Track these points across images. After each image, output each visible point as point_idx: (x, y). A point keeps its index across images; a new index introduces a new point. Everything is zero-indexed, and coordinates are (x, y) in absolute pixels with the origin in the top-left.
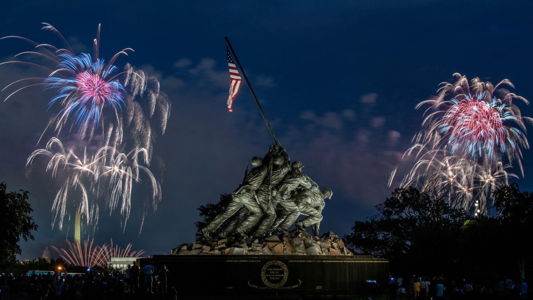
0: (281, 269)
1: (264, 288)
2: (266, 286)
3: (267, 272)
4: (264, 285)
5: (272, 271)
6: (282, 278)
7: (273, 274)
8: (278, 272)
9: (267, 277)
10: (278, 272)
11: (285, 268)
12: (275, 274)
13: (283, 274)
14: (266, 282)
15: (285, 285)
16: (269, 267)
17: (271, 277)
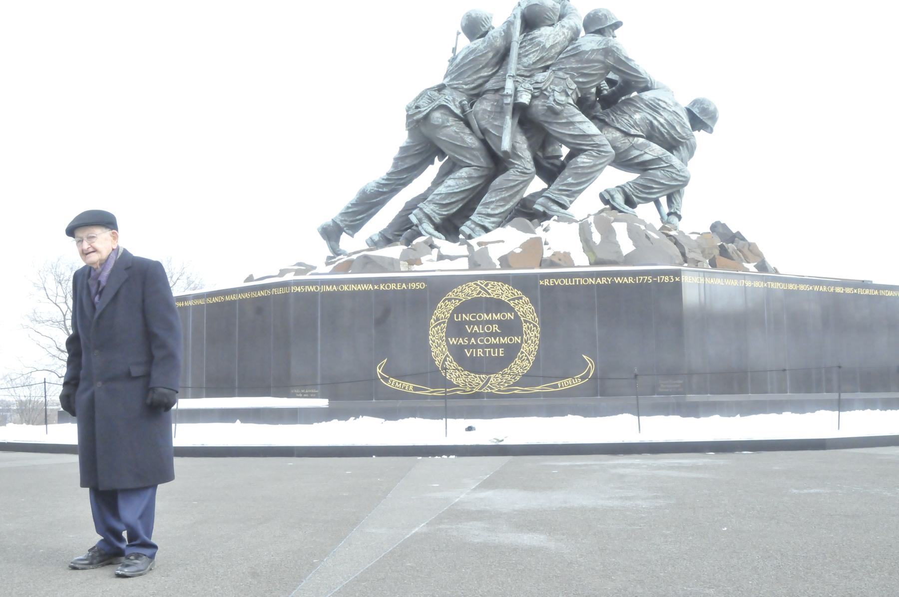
0: (509, 316)
2: (448, 384)
3: (456, 328)
5: (477, 323)
6: (512, 351)
7: (476, 335)
8: (495, 328)
9: (451, 348)
10: (495, 328)
11: (525, 308)
13: (520, 333)
15: (529, 379)
16: (458, 310)
17: (469, 347)
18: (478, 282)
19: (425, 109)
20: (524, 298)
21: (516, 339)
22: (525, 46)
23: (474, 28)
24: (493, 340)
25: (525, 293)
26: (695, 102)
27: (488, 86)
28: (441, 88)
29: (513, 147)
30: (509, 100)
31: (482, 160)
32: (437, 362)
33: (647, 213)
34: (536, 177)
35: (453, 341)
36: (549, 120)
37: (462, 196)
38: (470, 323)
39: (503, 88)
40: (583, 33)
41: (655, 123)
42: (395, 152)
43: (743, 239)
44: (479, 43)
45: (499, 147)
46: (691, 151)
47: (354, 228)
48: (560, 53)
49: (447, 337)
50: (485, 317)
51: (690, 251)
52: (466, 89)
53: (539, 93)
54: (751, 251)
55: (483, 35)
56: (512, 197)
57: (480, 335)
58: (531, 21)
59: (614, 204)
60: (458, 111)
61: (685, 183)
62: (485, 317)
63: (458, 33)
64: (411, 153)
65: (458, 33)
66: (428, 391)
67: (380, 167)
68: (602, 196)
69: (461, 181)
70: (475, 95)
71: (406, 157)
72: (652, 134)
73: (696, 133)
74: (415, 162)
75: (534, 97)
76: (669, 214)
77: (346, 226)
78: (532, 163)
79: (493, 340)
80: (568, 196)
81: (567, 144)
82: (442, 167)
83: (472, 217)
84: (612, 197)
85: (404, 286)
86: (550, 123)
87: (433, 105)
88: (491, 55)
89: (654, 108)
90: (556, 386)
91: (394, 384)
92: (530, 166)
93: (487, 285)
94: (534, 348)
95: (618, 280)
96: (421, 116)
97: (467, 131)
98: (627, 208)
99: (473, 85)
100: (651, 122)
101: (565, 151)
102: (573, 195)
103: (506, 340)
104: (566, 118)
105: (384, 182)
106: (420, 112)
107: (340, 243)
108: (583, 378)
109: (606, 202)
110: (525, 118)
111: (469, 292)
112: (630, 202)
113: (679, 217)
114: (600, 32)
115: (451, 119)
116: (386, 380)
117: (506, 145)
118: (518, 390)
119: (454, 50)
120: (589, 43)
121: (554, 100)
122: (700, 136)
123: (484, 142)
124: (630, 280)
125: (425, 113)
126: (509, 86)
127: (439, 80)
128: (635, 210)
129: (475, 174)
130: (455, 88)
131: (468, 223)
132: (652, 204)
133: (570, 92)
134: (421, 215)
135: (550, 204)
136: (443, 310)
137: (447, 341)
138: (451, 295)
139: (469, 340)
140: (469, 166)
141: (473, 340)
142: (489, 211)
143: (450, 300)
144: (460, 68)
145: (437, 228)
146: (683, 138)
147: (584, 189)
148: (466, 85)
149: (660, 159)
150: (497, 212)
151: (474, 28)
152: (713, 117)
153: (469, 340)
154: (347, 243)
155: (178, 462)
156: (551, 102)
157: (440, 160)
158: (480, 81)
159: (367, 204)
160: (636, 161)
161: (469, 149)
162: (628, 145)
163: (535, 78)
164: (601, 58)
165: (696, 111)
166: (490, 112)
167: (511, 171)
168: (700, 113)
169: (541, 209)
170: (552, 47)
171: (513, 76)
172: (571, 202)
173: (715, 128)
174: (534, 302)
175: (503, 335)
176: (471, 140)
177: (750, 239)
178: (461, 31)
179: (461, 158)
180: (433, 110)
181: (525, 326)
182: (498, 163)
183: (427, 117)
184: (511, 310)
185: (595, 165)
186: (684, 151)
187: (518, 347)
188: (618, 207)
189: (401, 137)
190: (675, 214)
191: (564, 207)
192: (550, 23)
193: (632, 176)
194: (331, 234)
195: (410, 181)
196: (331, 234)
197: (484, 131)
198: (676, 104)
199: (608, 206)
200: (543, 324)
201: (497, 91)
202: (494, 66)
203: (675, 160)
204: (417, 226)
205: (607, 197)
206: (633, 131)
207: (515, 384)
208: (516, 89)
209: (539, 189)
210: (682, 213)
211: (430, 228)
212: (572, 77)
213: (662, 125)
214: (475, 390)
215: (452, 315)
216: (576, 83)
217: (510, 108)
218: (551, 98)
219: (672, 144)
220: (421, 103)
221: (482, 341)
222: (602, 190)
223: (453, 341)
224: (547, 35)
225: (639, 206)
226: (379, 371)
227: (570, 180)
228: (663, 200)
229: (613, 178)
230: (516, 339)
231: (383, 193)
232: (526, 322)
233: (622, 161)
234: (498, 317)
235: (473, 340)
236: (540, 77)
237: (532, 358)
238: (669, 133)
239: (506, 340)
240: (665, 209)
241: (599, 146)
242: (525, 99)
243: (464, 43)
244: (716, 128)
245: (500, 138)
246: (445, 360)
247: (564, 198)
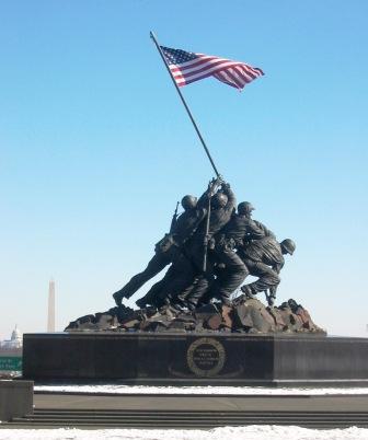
3: (196, 354)
6: (216, 362)
11: (220, 348)
25: (221, 342)
33: (261, 297)
67: (142, 267)
72: (265, 260)
89: (266, 248)
91: (177, 374)
112: (254, 293)
122: (286, 257)
136: (192, 348)
144: (178, 225)
152: (292, 249)
154: (126, 302)
155: (35, 396)
174: (224, 346)
196: (118, 296)
229: (251, 279)
233: (254, 271)
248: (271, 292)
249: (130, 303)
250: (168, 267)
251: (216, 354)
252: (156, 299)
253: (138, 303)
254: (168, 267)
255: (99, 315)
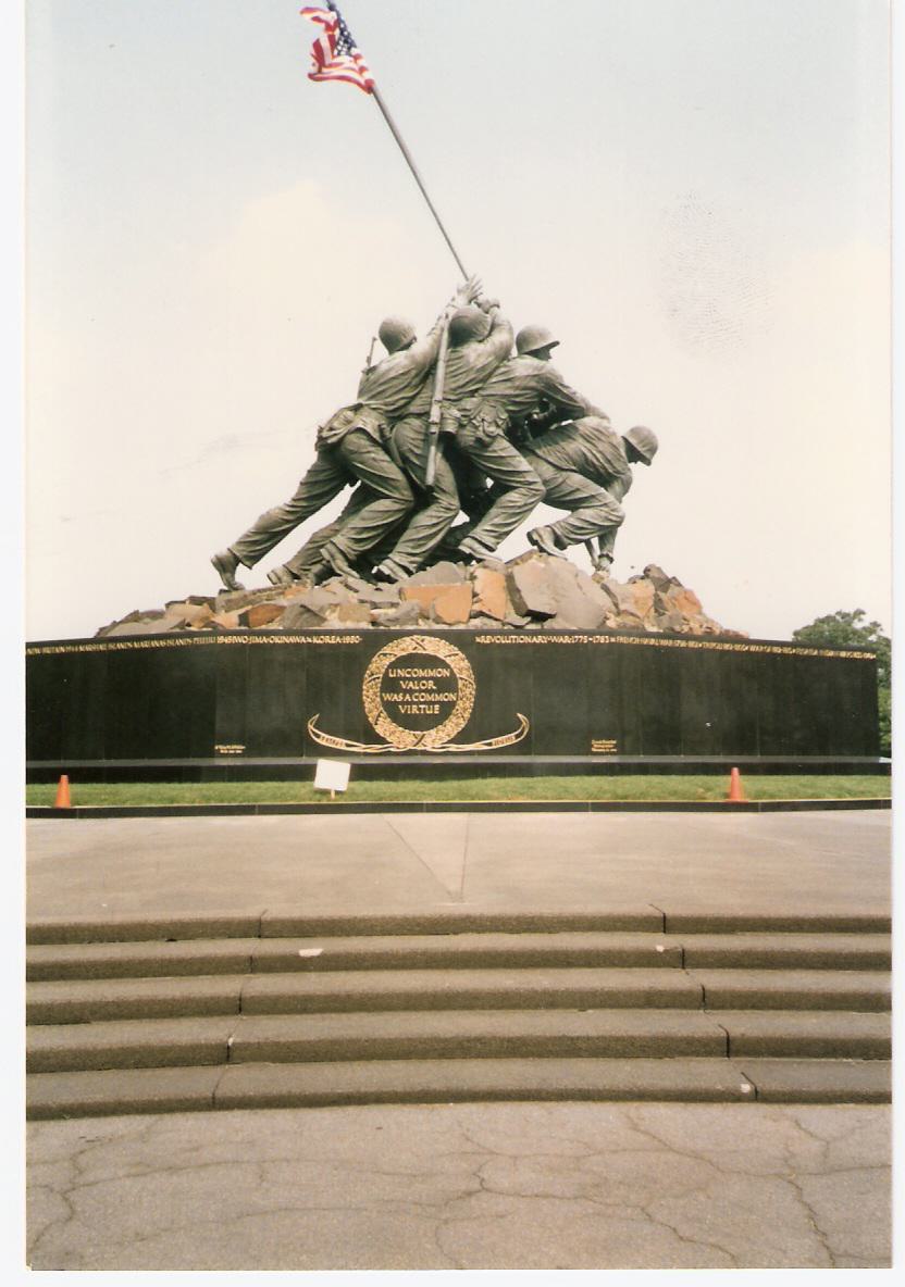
1: (375, 748)
2: (381, 740)
3: (390, 685)
4: (372, 737)
5: (412, 679)
6: (447, 709)
7: (411, 691)
11: (459, 664)
12: (420, 691)
13: (455, 690)
14: (384, 727)
15: (462, 737)
16: (393, 666)
17: (403, 703)
18: (415, 637)
19: (342, 431)
20: (461, 654)
21: (452, 697)
22: (452, 365)
23: (393, 339)
24: (429, 698)
26: (634, 431)
27: (413, 408)
28: (357, 408)
29: (437, 479)
30: (434, 429)
31: (407, 494)
32: (370, 719)
33: (577, 554)
34: (461, 512)
35: (387, 697)
36: (478, 452)
37: (380, 531)
38: (405, 679)
39: (427, 414)
40: (514, 352)
41: (589, 455)
42: (302, 474)
43: (679, 585)
44: (401, 358)
45: (423, 480)
46: (626, 486)
47: (253, 559)
48: (490, 375)
49: (381, 692)
50: (421, 673)
51: (623, 600)
52: (387, 412)
53: (465, 421)
54: (686, 598)
55: (407, 346)
56: (436, 534)
57: (416, 691)
58: (460, 333)
59: (543, 545)
60: (376, 436)
61: (619, 524)
62: (421, 673)
63: (375, 339)
64: (321, 477)
65: (375, 339)
66: (360, 748)
67: (283, 490)
68: (529, 535)
69: (379, 514)
70: (396, 416)
71: (311, 483)
73: (632, 465)
74: (326, 488)
75: (462, 426)
76: (600, 557)
77: (245, 556)
78: (457, 497)
79: (429, 698)
80: (496, 537)
81: (492, 478)
82: (354, 495)
83: (395, 556)
84: (540, 536)
85: (338, 639)
86: (476, 455)
87: (350, 427)
88: (413, 373)
90: (490, 744)
92: (456, 502)
93: (423, 641)
94: (469, 704)
95: (554, 639)
96: (334, 440)
97: (387, 458)
98: (556, 551)
99: (392, 408)
100: (584, 454)
101: (489, 483)
102: (501, 536)
103: (441, 697)
104: (495, 451)
105: (288, 509)
106: (335, 435)
107: (236, 576)
108: (517, 736)
109: (534, 543)
110: (448, 443)
111: (406, 646)
112: (560, 544)
113: (611, 560)
114: (535, 354)
115: (368, 443)
116: (318, 736)
117: (430, 480)
118: (453, 748)
119: (369, 360)
120: (524, 366)
121: (484, 431)
122: (637, 468)
123: (404, 471)
124: (566, 640)
125: (339, 436)
126: (435, 415)
127: (354, 400)
128: (564, 551)
129: (397, 507)
130: (374, 409)
131: (387, 561)
132: (583, 544)
133: (500, 423)
134: (334, 550)
135: (476, 546)
136: (379, 664)
137: (382, 698)
138: (386, 650)
139: (404, 696)
140: (388, 497)
141: (408, 697)
142: (410, 551)
143: (385, 655)
145: (352, 565)
146: (618, 472)
147: (512, 531)
148: (386, 405)
149: (593, 496)
150: (418, 551)
151: (393, 339)
152: (653, 450)
153: (404, 696)
154: (242, 574)
156: (480, 434)
157: (352, 486)
158: (403, 402)
159: (268, 535)
160: (568, 498)
161: (384, 480)
162: (560, 480)
163: (463, 403)
164: (533, 384)
165: (633, 441)
166: (413, 439)
167: (434, 507)
168: (639, 443)
169: (468, 551)
170: (483, 368)
171: (440, 402)
172: (498, 543)
173: (654, 460)
175: (439, 692)
176: (392, 471)
177: (687, 585)
178: (377, 337)
179: (380, 489)
180: (349, 433)
181: (460, 683)
182: (423, 497)
183: (341, 441)
184: (447, 666)
185: (526, 505)
186: (617, 487)
187: (452, 704)
188: (546, 548)
189: (311, 457)
190: (607, 556)
191: (491, 550)
192: (481, 338)
193: (563, 514)
194: (226, 566)
195: (319, 509)
197: (405, 460)
198: (614, 434)
199: (536, 547)
200: (478, 681)
201: (418, 415)
202: (416, 386)
203: (608, 496)
204: (328, 562)
205: (535, 537)
206: (564, 465)
207: (449, 742)
208: (442, 414)
209: (460, 523)
210: (614, 555)
211: (344, 566)
212: (504, 404)
213: (597, 459)
214: (409, 747)
215: (387, 670)
216: (508, 411)
217: (436, 436)
218: (481, 429)
219: (604, 478)
220: (336, 424)
221: (416, 697)
222: (530, 529)
223: (387, 697)
224: (476, 353)
225: (569, 547)
226: (310, 727)
227: (497, 521)
228: (595, 542)
229: (545, 516)
230: (452, 697)
231: (288, 521)
232: (461, 679)
233: (554, 499)
234: (432, 673)
235: (408, 697)
236: (469, 403)
237: (467, 715)
238: (605, 468)
239: (441, 697)
240: (597, 552)
241: (531, 483)
242: (451, 428)
243: (381, 351)
244: (654, 460)
245: (424, 470)
246: (379, 716)
247: (494, 540)
248: (602, 544)
249: (252, 578)
250: (346, 493)
251: (447, 684)
252: (316, 566)
253: (275, 578)
254: (346, 493)
255: (168, 605)
